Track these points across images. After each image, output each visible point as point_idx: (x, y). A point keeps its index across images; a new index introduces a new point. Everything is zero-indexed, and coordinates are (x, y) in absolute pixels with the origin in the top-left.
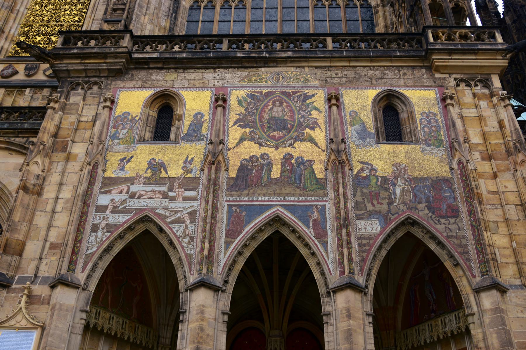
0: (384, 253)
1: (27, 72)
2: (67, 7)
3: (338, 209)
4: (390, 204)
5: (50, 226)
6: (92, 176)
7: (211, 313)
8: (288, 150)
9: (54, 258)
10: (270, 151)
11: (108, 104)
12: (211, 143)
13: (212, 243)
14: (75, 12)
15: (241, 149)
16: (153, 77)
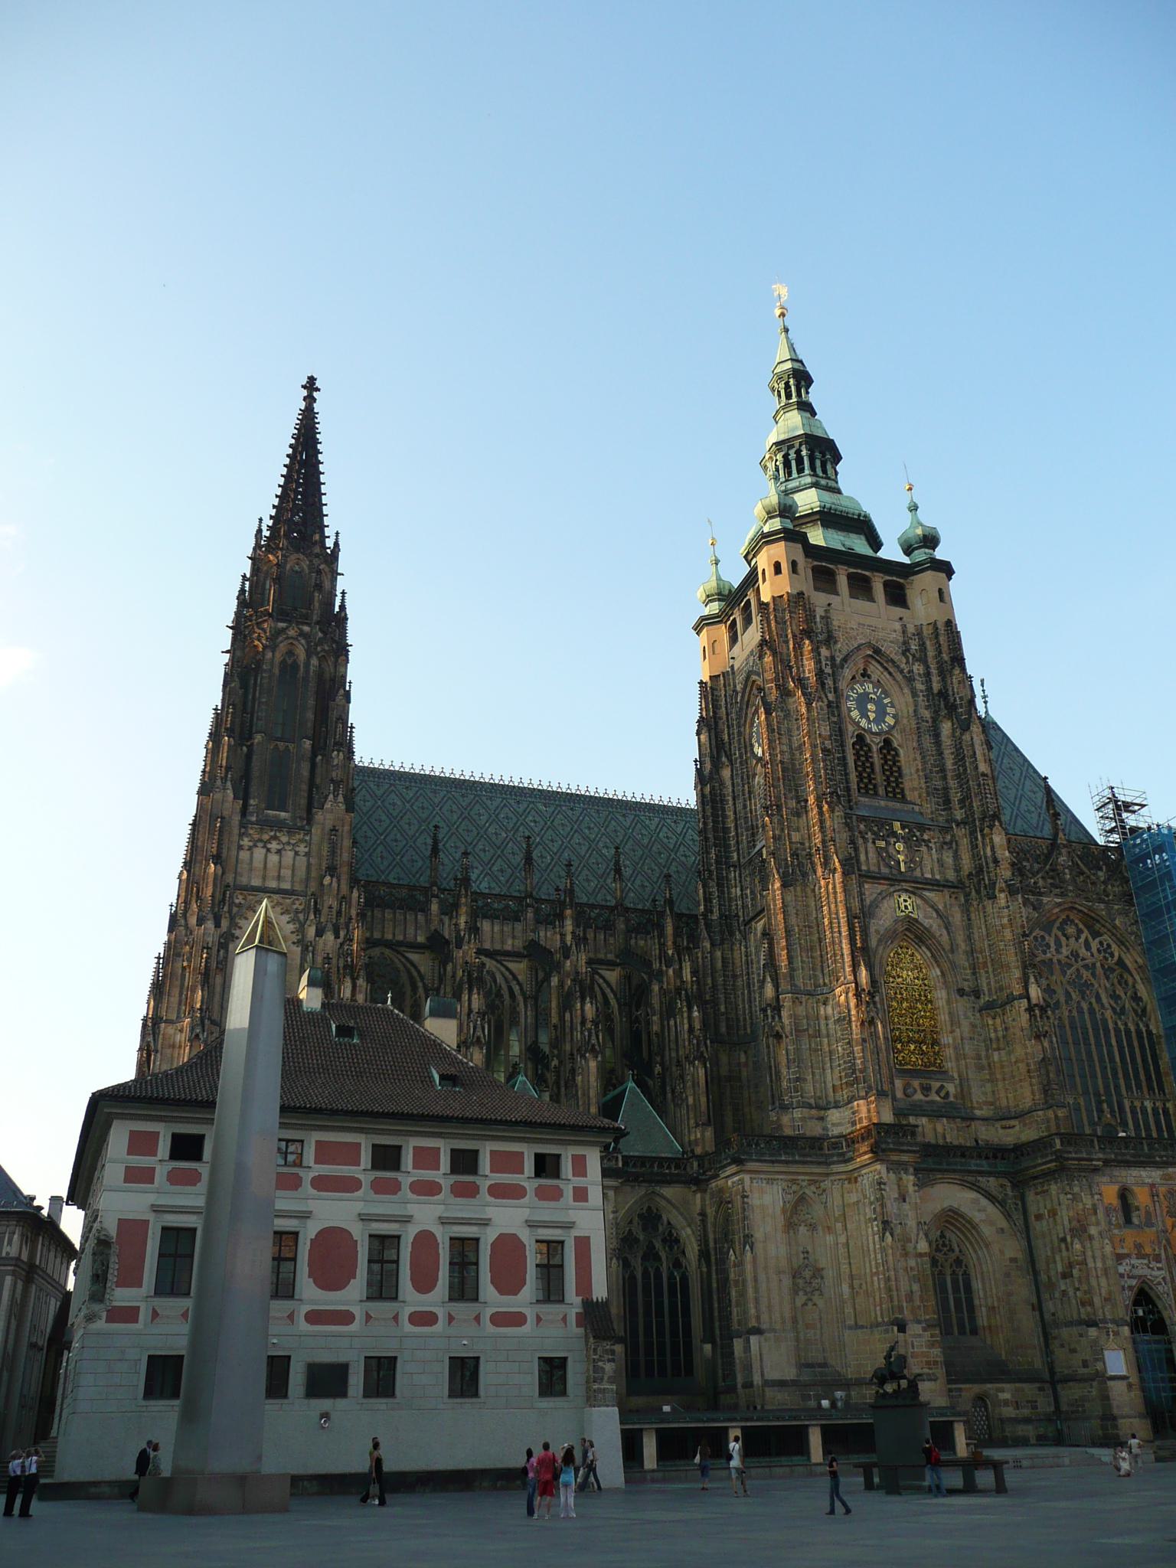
2: (919, 1006)
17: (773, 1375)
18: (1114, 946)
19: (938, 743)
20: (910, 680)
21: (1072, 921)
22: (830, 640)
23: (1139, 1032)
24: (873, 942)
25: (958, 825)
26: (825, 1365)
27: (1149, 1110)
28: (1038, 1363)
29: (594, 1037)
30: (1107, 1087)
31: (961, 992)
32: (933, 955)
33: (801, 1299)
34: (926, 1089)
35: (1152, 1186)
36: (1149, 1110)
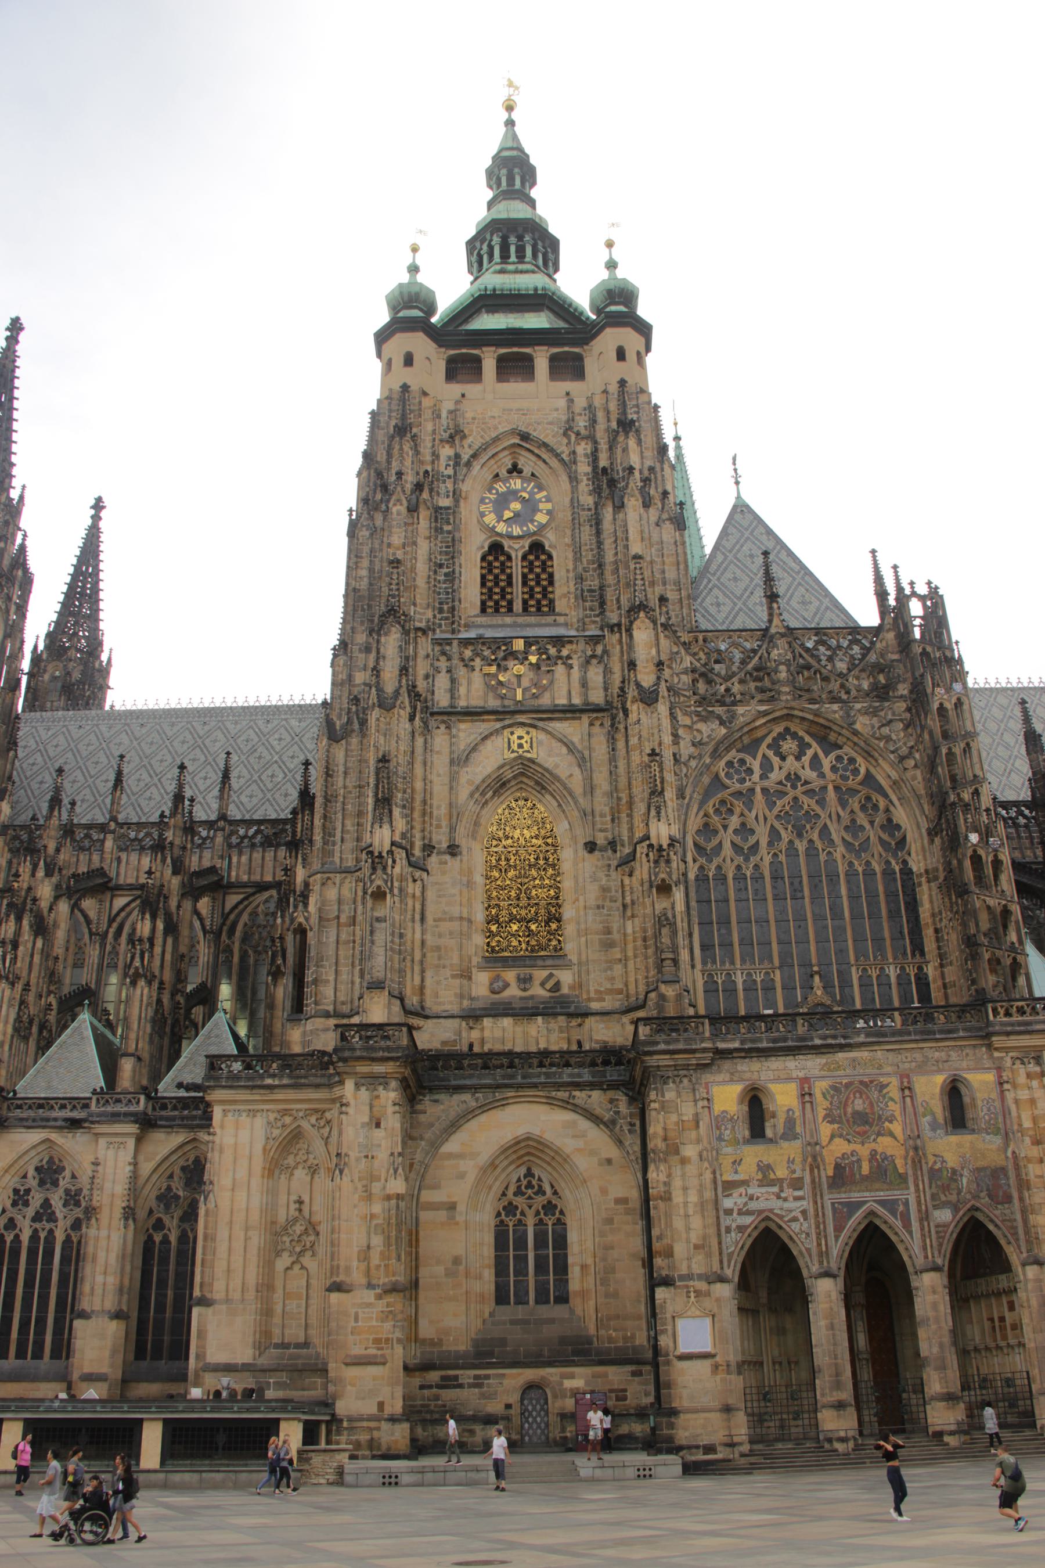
0: (955, 1235)
1: (522, 986)
2: (534, 872)
3: (919, 1203)
4: (959, 1194)
5: (688, 1229)
6: (715, 1181)
7: (834, 1295)
8: (873, 1145)
9: (700, 1257)
10: (857, 1147)
11: (705, 1103)
12: (809, 1144)
13: (826, 1237)
14: (547, 881)
15: (832, 1147)
16: (739, 1068)
17: (216, 1355)
18: (859, 759)
19: (598, 533)
20: (569, 465)
21: (795, 736)
22: (456, 435)
23: (888, 873)
24: (463, 793)
25: (612, 631)
26: (306, 1345)
27: (893, 979)
28: (641, 1339)
29: (137, 959)
30: (823, 953)
31: (591, 847)
32: (560, 805)
33: (283, 1262)
34: (525, 981)
35: (805, 1081)
36: (893, 979)
